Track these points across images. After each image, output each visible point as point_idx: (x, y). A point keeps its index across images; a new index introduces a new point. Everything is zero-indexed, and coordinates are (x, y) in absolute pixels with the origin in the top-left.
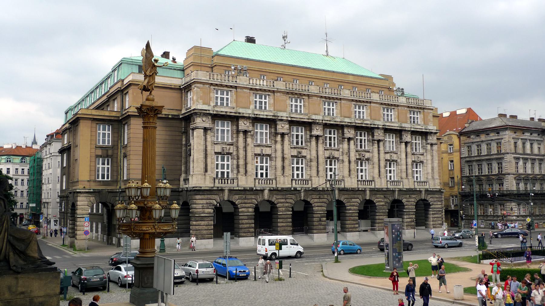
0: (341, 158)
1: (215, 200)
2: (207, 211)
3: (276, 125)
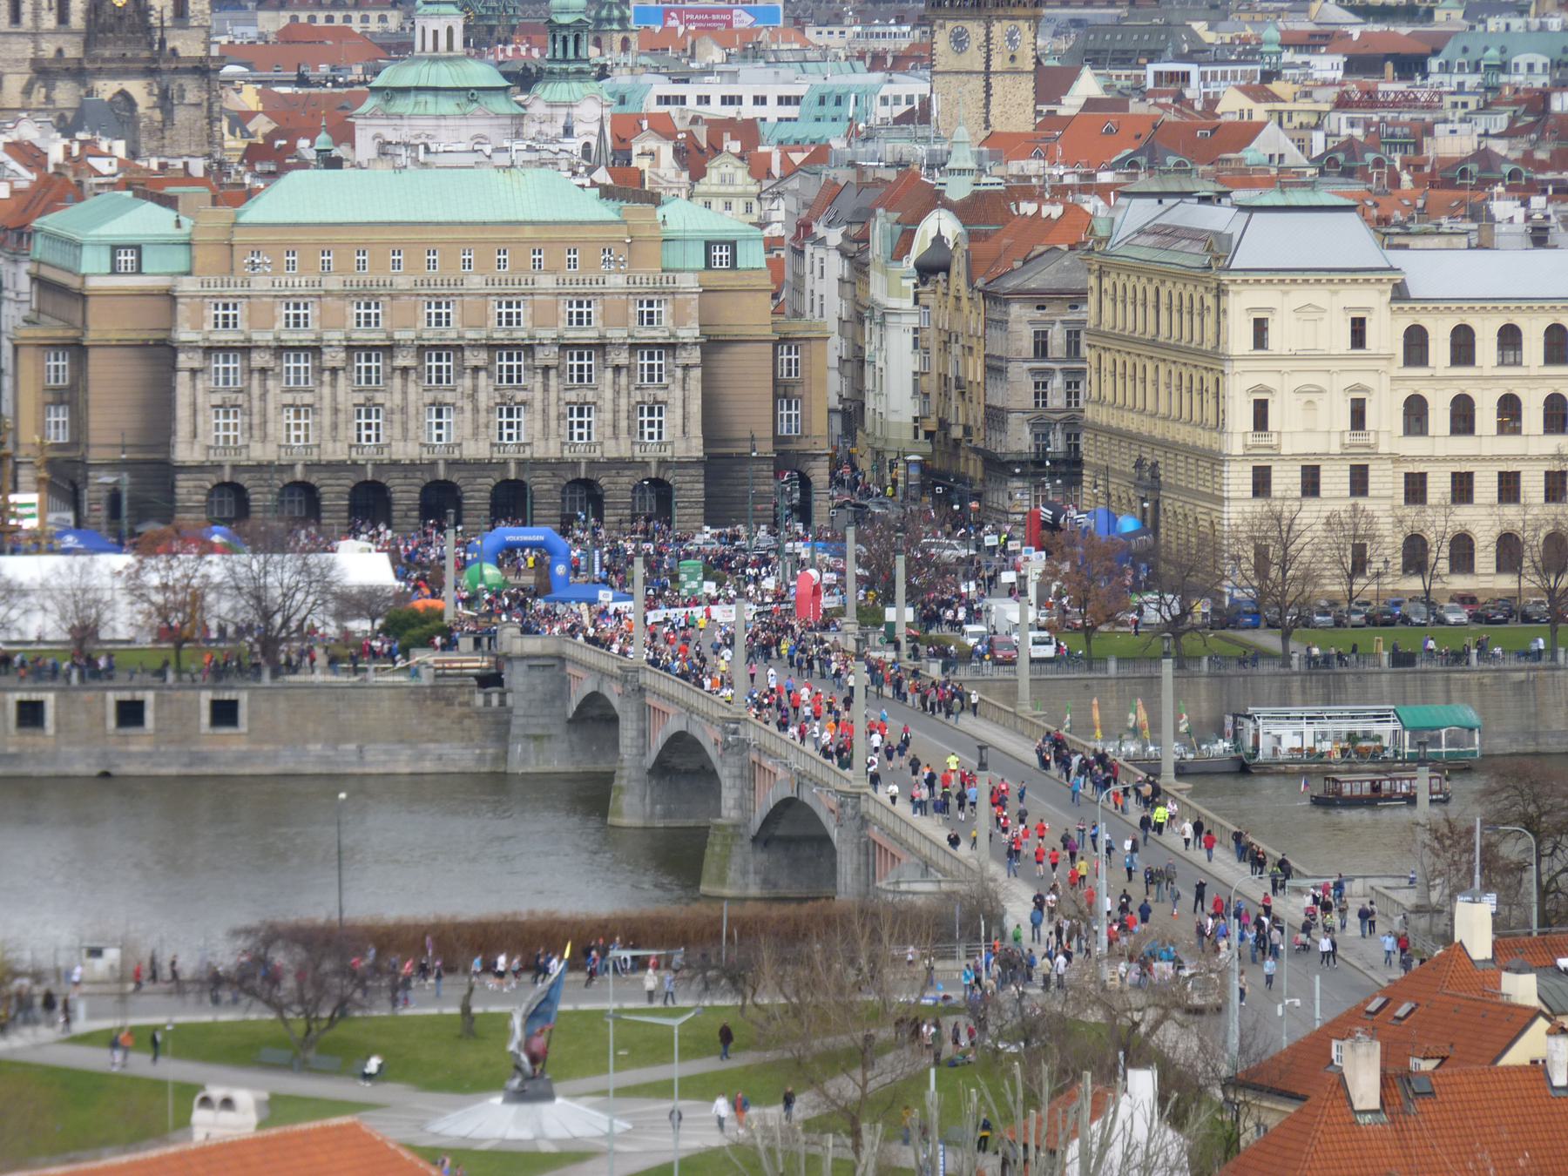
0: (459, 404)
1: (209, 481)
2: (196, 497)
3: (321, 353)
